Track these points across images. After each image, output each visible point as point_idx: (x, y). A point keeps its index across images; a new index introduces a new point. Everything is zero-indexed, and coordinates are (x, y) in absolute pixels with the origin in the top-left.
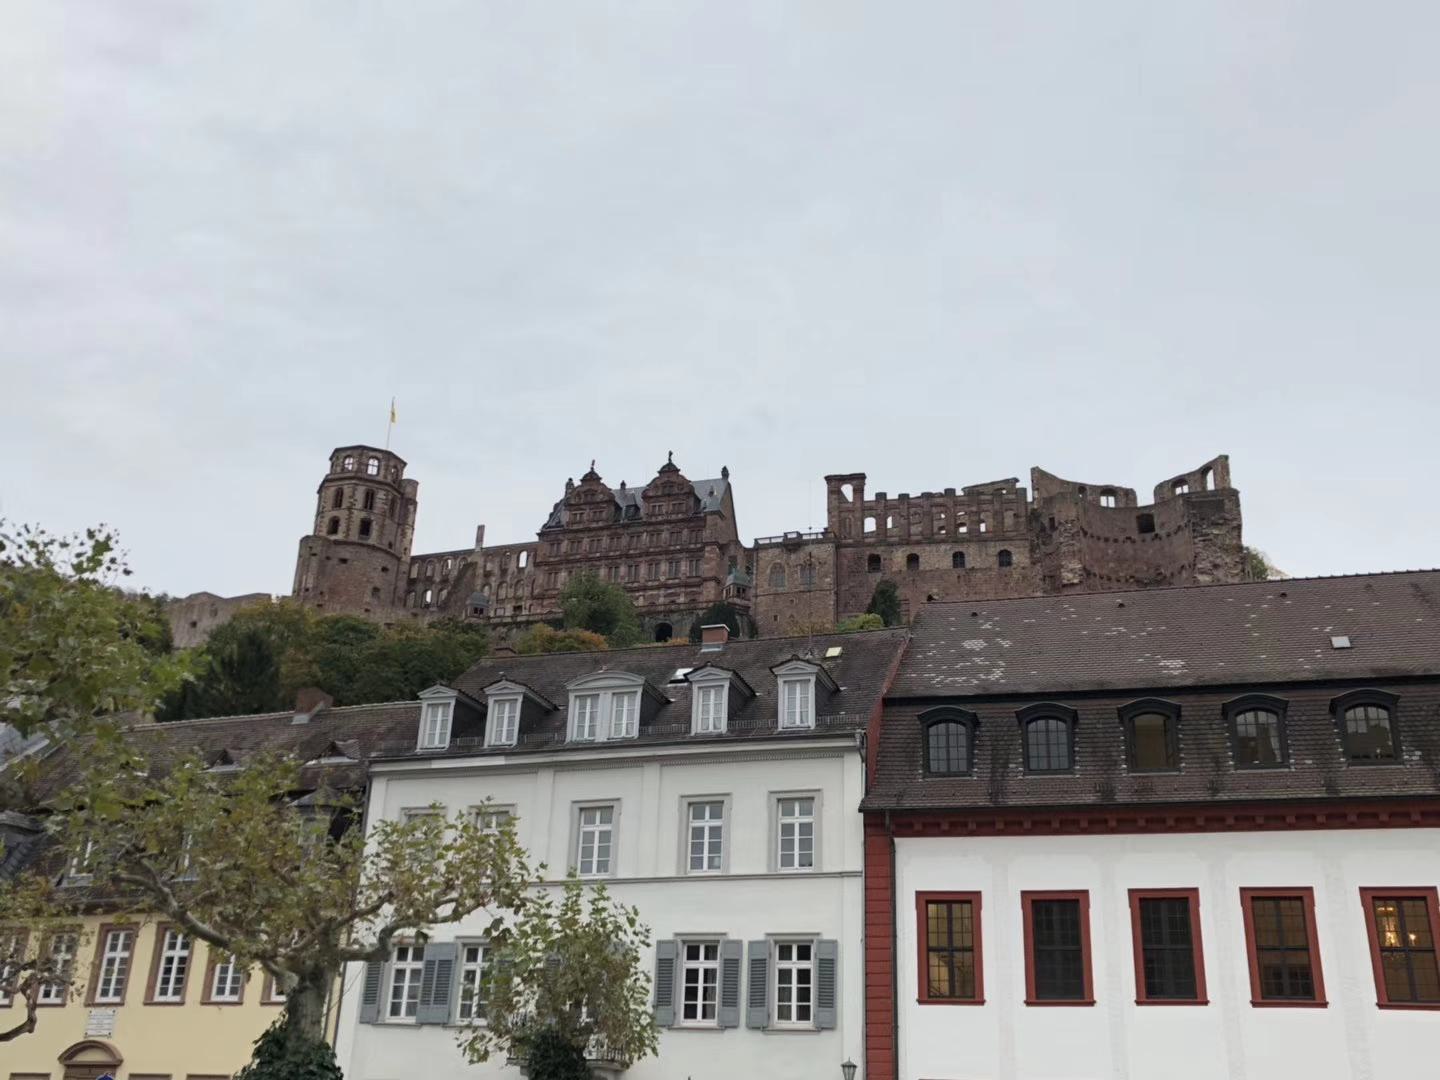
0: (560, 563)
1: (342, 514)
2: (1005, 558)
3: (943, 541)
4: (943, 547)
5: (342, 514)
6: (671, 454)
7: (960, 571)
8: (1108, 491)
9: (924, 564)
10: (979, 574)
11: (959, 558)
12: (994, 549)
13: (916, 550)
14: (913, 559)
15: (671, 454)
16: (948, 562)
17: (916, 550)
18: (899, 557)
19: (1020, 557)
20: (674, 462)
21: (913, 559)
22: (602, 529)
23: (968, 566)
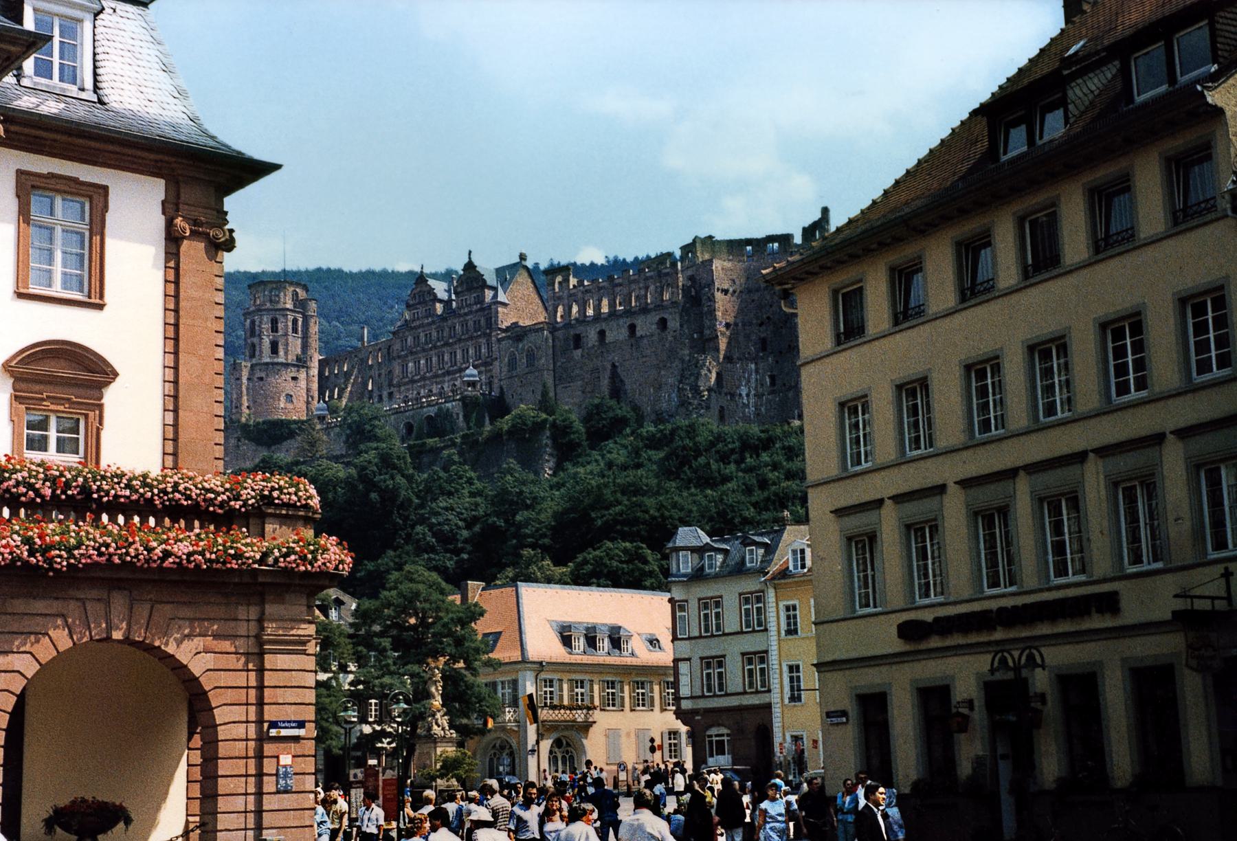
0: (406, 356)
1: (256, 340)
2: (663, 323)
3: (621, 316)
4: (621, 321)
5: (256, 340)
6: (470, 252)
7: (633, 341)
8: (771, 239)
9: (610, 337)
10: (645, 341)
11: (632, 328)
12: (655, 317)
13: (604, 326)
14: (602, 333)
15: (470, 252)
16: (624, 333)
17: (604, 326)
18: (592, 335)
19: (674, 323)
20: (476, 262)
21: (602, 333)
22: (430, 324)
23: (638, 334)
